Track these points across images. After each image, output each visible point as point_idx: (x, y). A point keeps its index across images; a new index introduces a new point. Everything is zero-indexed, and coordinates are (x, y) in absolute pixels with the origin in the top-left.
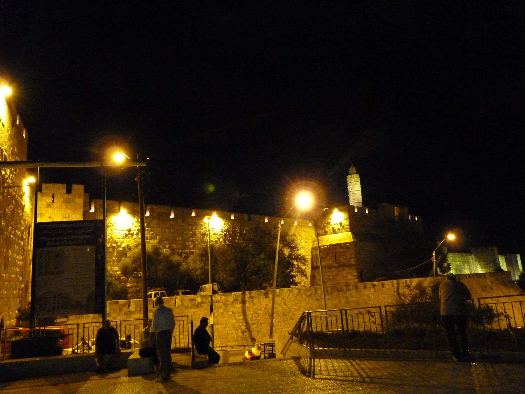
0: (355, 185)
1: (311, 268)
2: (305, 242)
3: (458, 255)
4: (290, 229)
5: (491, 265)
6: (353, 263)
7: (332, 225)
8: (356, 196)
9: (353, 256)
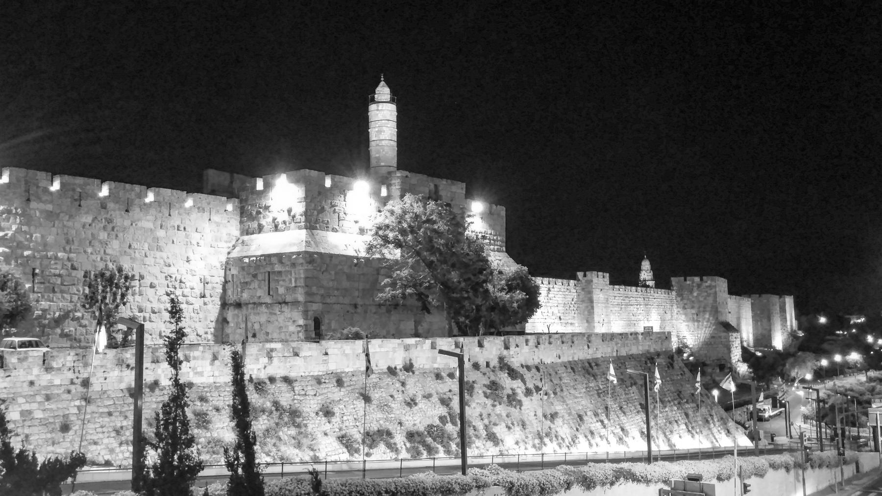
0: (384, 128)
1: (219, 303)
3: (636, 291)
4: (170, 215)
5: (707, 316)
8: (383, 151)
9: (301, 283)
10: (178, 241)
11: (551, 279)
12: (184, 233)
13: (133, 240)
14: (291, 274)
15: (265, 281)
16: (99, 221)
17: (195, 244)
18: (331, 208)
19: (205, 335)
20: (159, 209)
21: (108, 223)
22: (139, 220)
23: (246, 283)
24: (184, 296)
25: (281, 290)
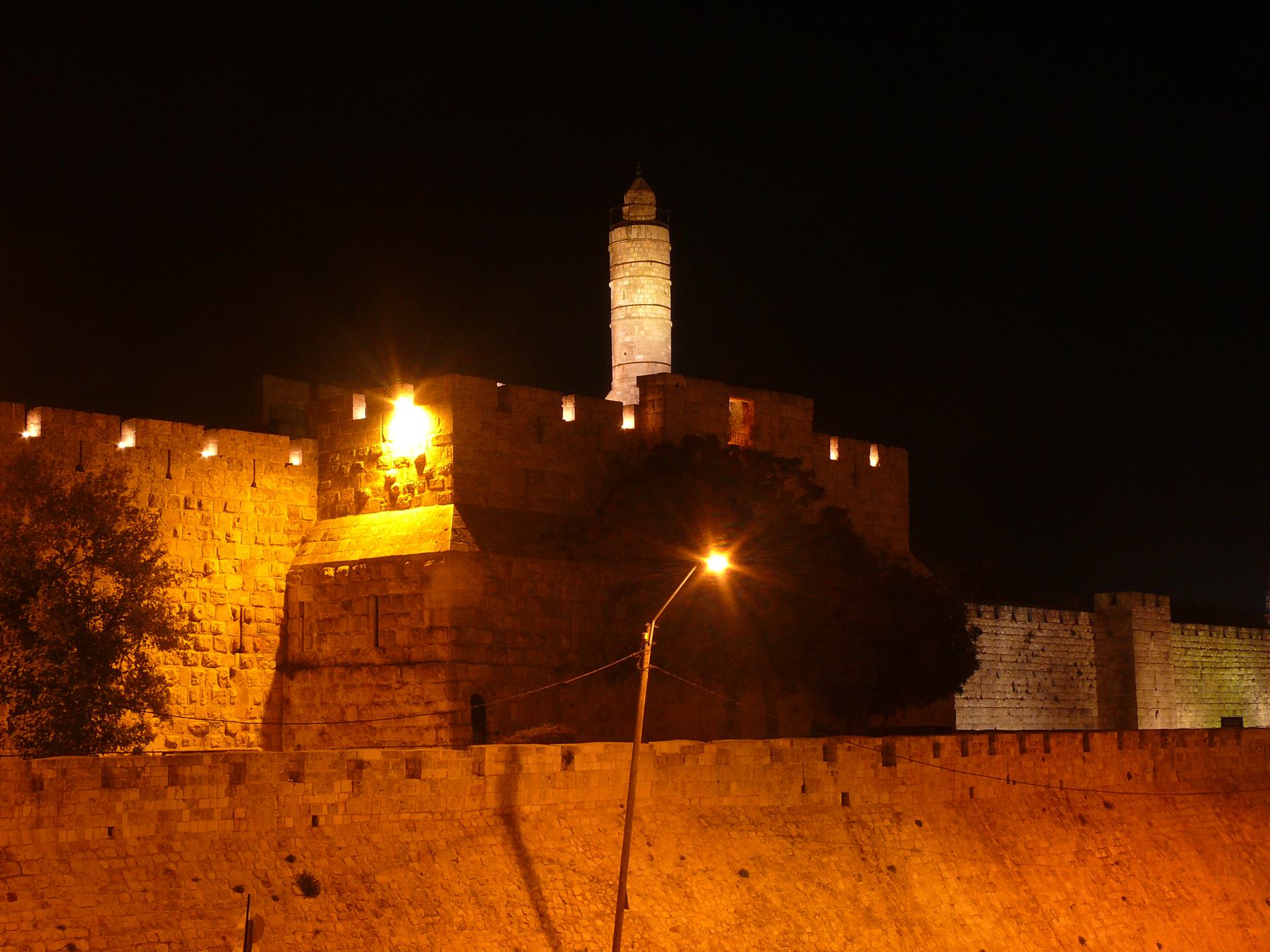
0: (643, 280)
2: (253, 540)
3: (1238, 637)
4: (169, 476)
6: (442, 653)
7: (384, 467)
8: (641, 329)
11: (1034, 610)
15: (367, 616)
17: (222, 536)
19: (243, 734)
20: (145, 465)
23: (330, 620)
24: (197, 648)
25: (402, 637)
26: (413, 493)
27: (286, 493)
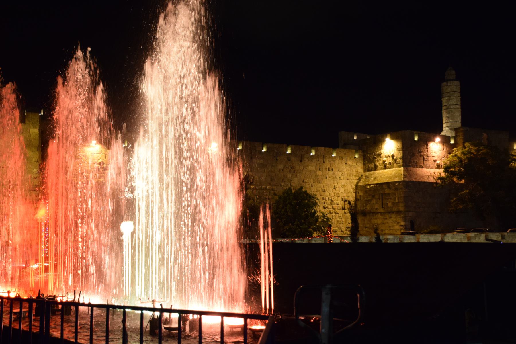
2: (346, 179)
4: (324, 162)
6: (401, 208)
7: (383, 157)
8: (452, 112)
10: (329, 177)
12: (332, 172)
13: (305, 178)
14: (395, 195)
16: (287, 168)
18: (418, 153)
19: (346, 232)
20: (318, 159)
21: (292, 168)
22: (307, 166)
23: (368, 200)
24: (333, 208)
25: (390, 204)
26: (391, 165)
27: (355, 165)
